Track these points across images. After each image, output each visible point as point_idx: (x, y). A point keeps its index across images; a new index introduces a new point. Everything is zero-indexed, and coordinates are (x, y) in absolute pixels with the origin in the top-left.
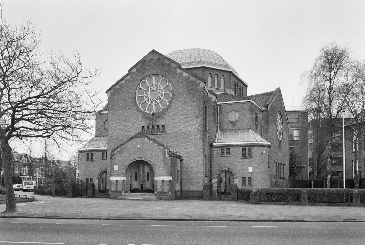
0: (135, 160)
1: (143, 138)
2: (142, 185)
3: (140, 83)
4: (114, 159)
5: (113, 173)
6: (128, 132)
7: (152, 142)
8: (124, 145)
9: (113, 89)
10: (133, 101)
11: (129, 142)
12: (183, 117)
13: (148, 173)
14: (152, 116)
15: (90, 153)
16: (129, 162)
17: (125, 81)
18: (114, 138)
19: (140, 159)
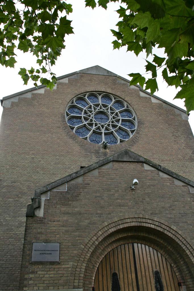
0: (121, 227)
1: (139, 166)
3: (74, 97)
5: (33, 272)
6: (43, 174)
7: (166, 176)
8: (80, 180)
9: (17, 97)
10: (60, 120)
11: (96, 172)
12: (166, 158)
14: (102, 150)
16: (100, 233)
17: (45, 91)
18: (5, 184)
19: (139, 224)
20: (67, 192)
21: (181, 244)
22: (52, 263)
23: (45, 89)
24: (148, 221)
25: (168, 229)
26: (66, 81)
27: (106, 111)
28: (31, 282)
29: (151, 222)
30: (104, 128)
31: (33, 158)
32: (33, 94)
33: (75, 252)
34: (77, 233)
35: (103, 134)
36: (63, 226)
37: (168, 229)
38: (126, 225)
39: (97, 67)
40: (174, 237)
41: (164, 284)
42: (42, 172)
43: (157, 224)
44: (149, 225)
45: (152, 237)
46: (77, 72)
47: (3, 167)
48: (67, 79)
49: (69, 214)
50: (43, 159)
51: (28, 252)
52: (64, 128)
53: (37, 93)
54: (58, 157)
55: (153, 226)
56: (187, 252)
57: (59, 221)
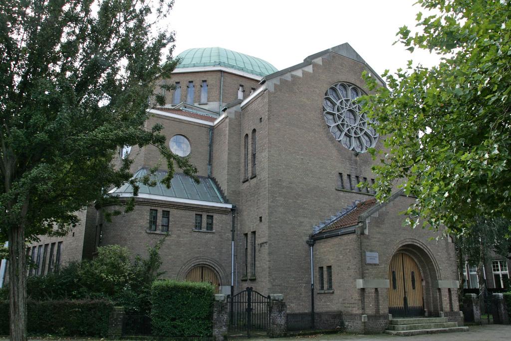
2: (405, 299)
4: (367, 237)
5: (367, 270)
8: (384, 209)
13: (413, 273)
15: (160, 210)
18: (284, 184)
19: (412, 243)
20: (378, 217)
21: (431, 257)
22: (375, 265)
23: (303, 71)
24: (418, 242)
25: (426, 247)
26: (319, 61)
27: (358, 114)
28: (367, 275)
29: (418, 242)
30: (348, 128)
31: (302, 159)
32: (293, 76)
33: (385, 258)
34: (385, 247)
35: (344, 133)
36: (378, 242)
37: (426, 247)
38: (406, 243)
39: (346, 46)
40: (428, 253)
41: (416, 280)
42: (311, 175)
43: (421, 244)
44: (416, 244)
45: (414, 250)
46: (328, 50)
47: (280, 166)
48: (321, 58)
49: (380, 233)
50: (310, 161)
51: (364, 258)
52: (324, 127)
53: (296, 75)
54: (321, 161)
55: (419, 245)
56: (433, 262)
57: (375, 238)
